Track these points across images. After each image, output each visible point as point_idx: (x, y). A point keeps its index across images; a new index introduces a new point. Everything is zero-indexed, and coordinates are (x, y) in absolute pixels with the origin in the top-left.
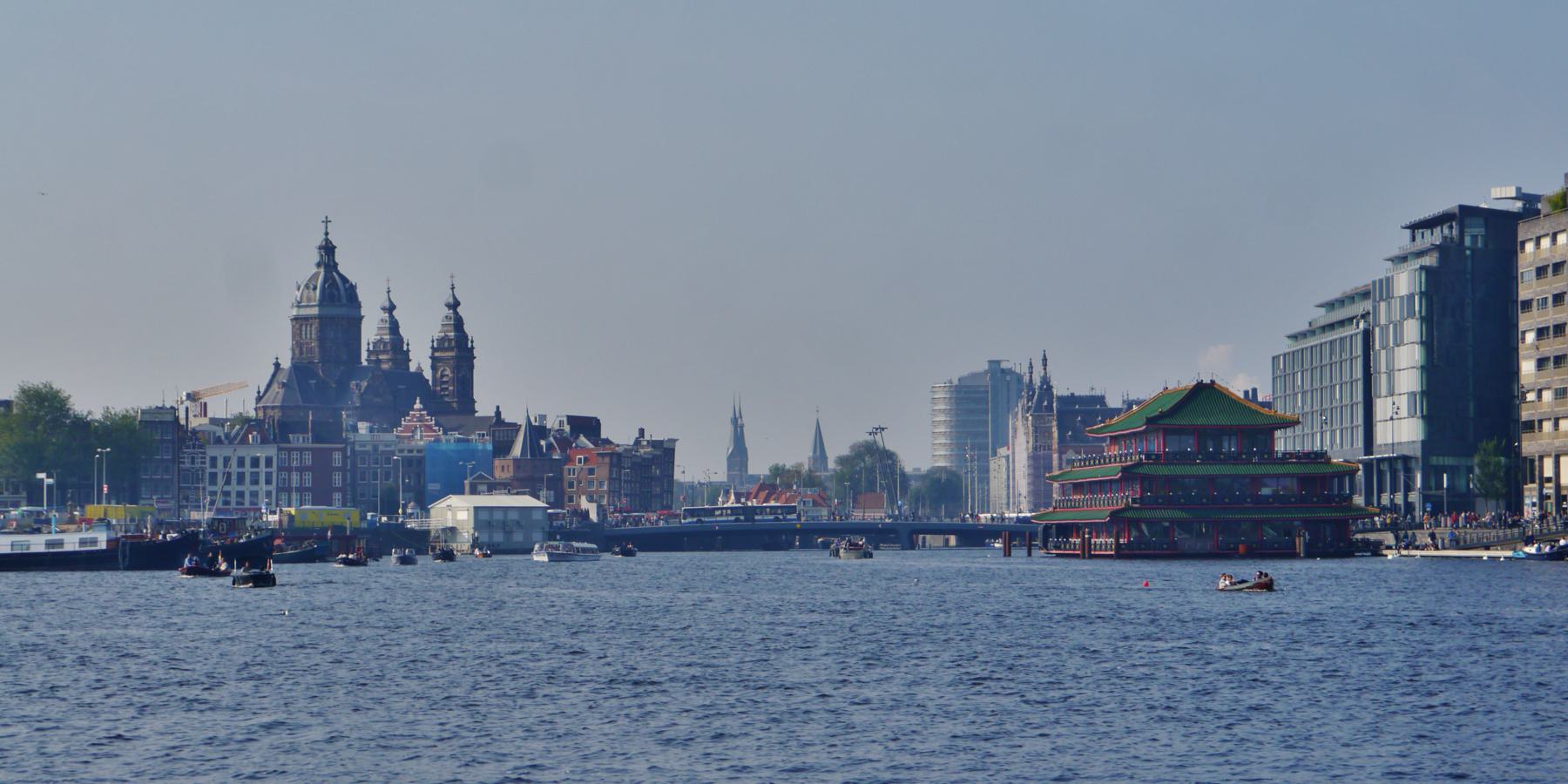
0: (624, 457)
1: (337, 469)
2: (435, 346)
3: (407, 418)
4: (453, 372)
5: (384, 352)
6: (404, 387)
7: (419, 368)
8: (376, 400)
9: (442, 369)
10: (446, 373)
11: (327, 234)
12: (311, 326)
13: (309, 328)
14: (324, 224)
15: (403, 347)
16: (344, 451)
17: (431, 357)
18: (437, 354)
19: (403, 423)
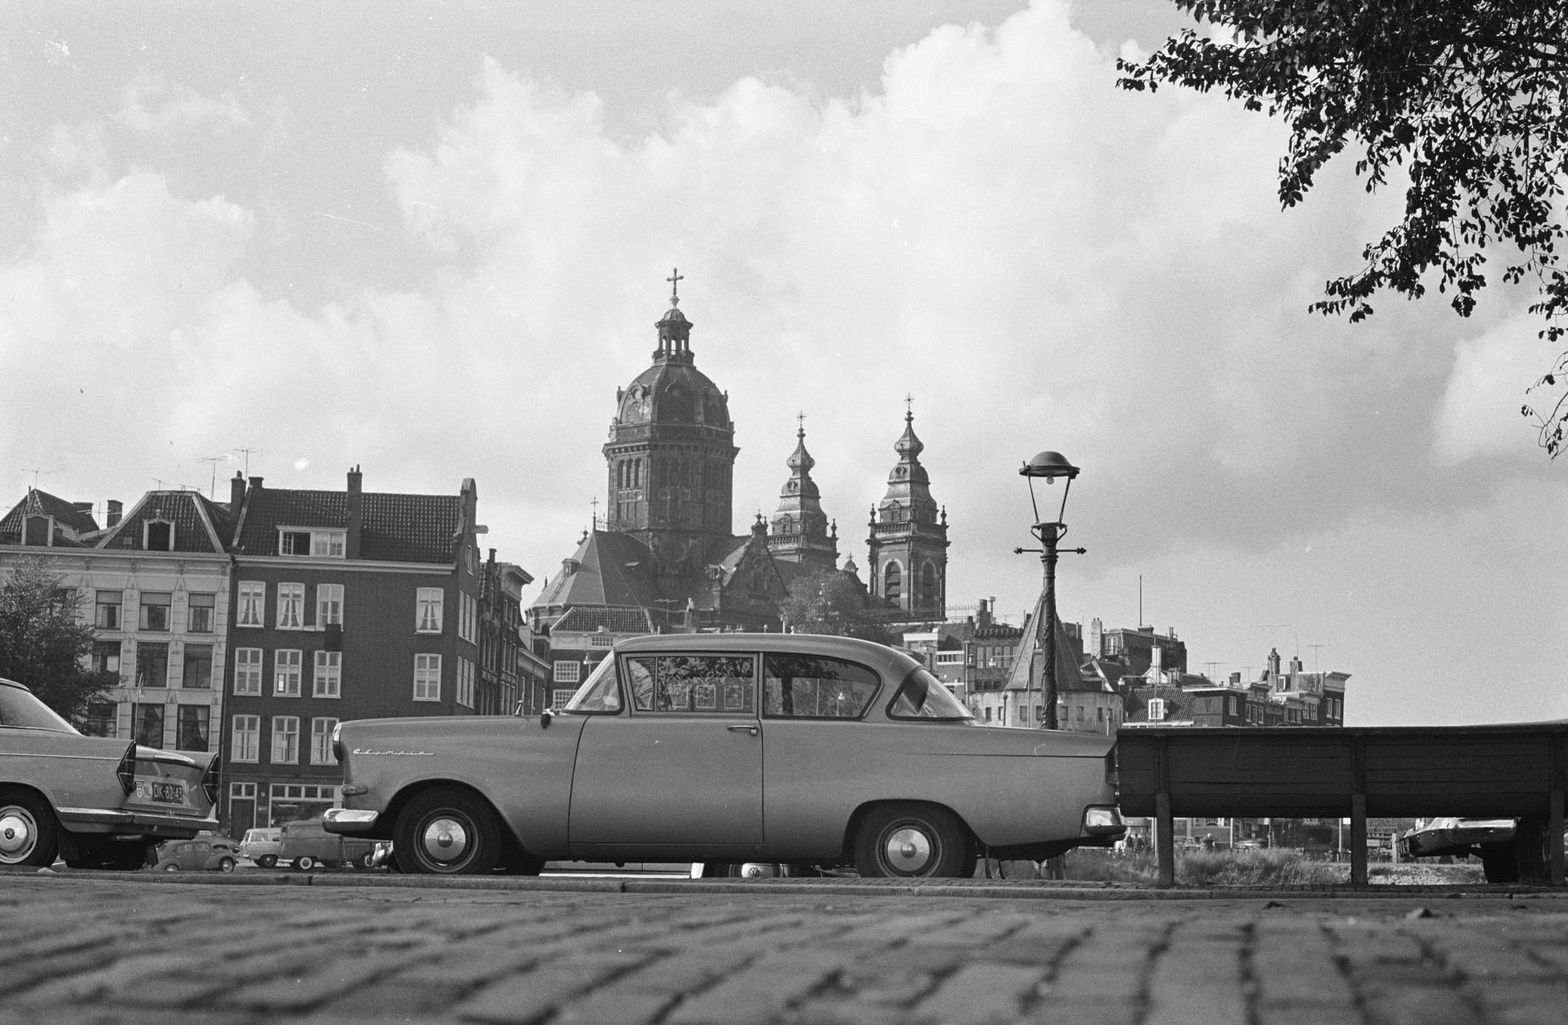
1: (429, 643)
2: (878, 519)
5: (787, 539)
7: (851, 564)
8: (753, 602)
11: (675, 301)
12: (638, 461)
13: (633, 469)
14: (672, 282)
16: (451, 586)
17: (868, 542)
18: (879, 536)
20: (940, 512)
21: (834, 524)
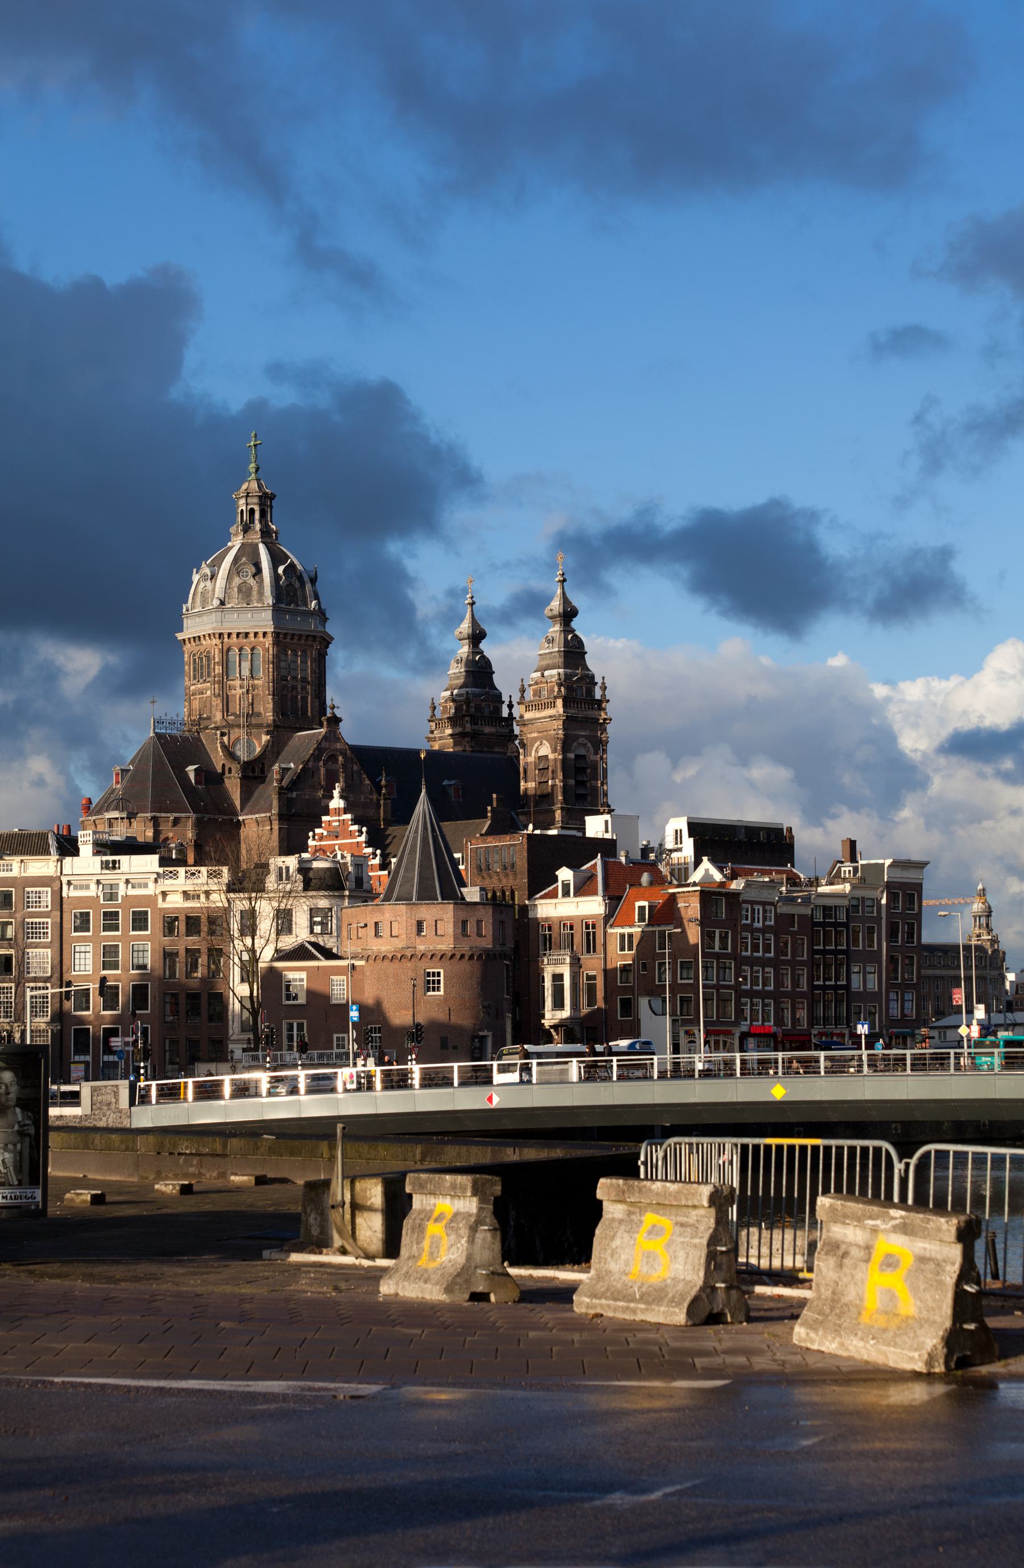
0: (752, 903)
3: (318, 831)
4: (554, 751)
6: (452, 782)
9: (538, 743)
10: (541, 753)
15: (499, 710)
19: (311, 842)
20: (599, 684)
21: (510, 702)
